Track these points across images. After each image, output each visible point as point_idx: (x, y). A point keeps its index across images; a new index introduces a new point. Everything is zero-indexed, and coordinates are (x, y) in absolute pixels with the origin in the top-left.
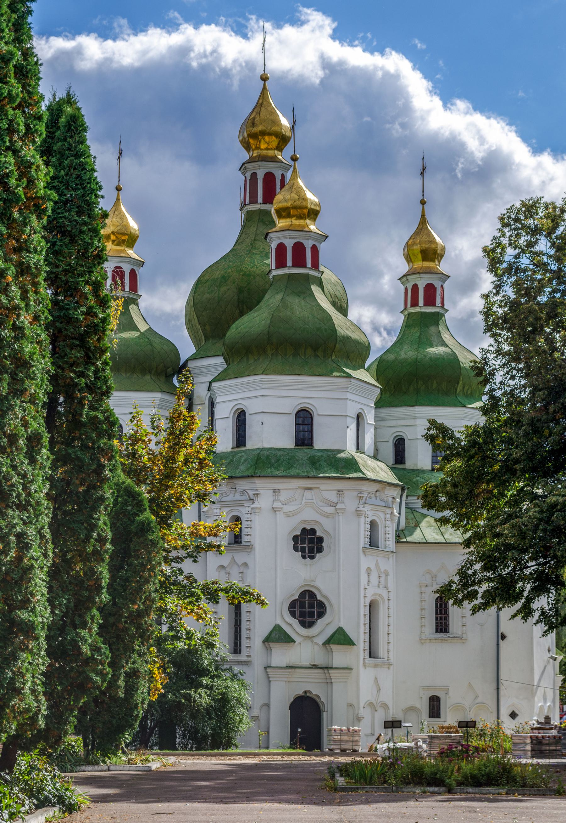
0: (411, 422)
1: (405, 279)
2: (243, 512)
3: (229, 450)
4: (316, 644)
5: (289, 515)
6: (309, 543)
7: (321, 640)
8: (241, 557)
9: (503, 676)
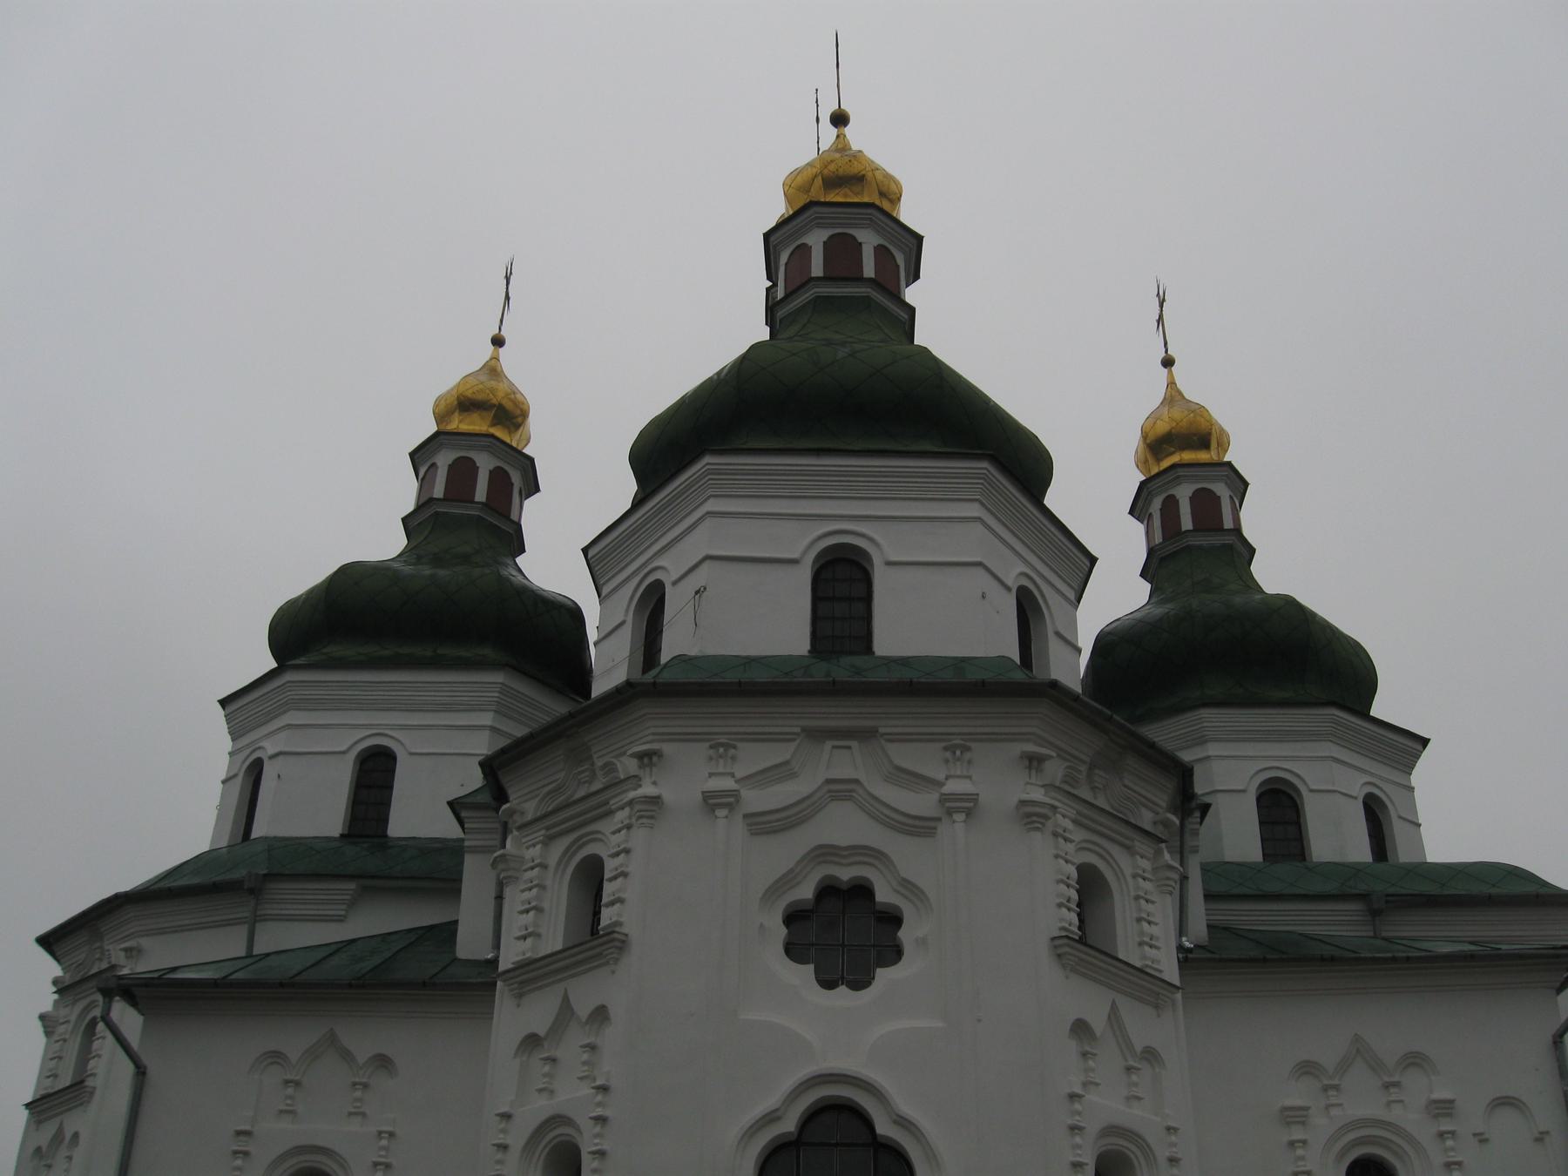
1: (1144, 495)
2: (607, 840)
8: (586, 992)
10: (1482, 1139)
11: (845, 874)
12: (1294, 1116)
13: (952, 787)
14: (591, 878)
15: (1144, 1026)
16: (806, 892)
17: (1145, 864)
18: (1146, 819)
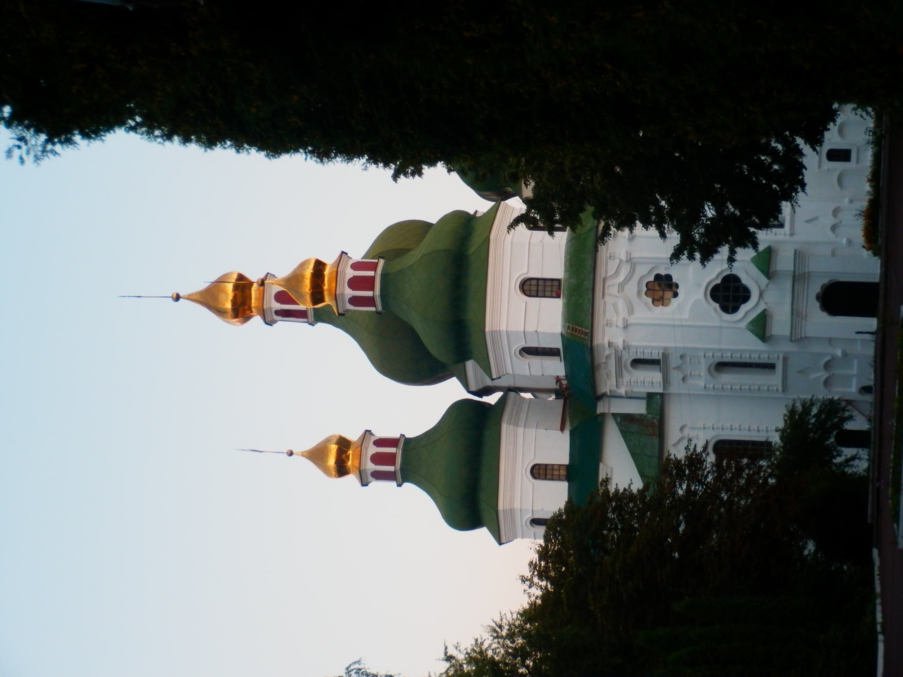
2: (628, 358)
3: (563, 364)
4: (767, 286)
5: (631, 311)
7: (764, 280)
8: (674, 361)
11: (645, 289)
13: (623, 257)
14: (637, 363)
16: (650, 300)
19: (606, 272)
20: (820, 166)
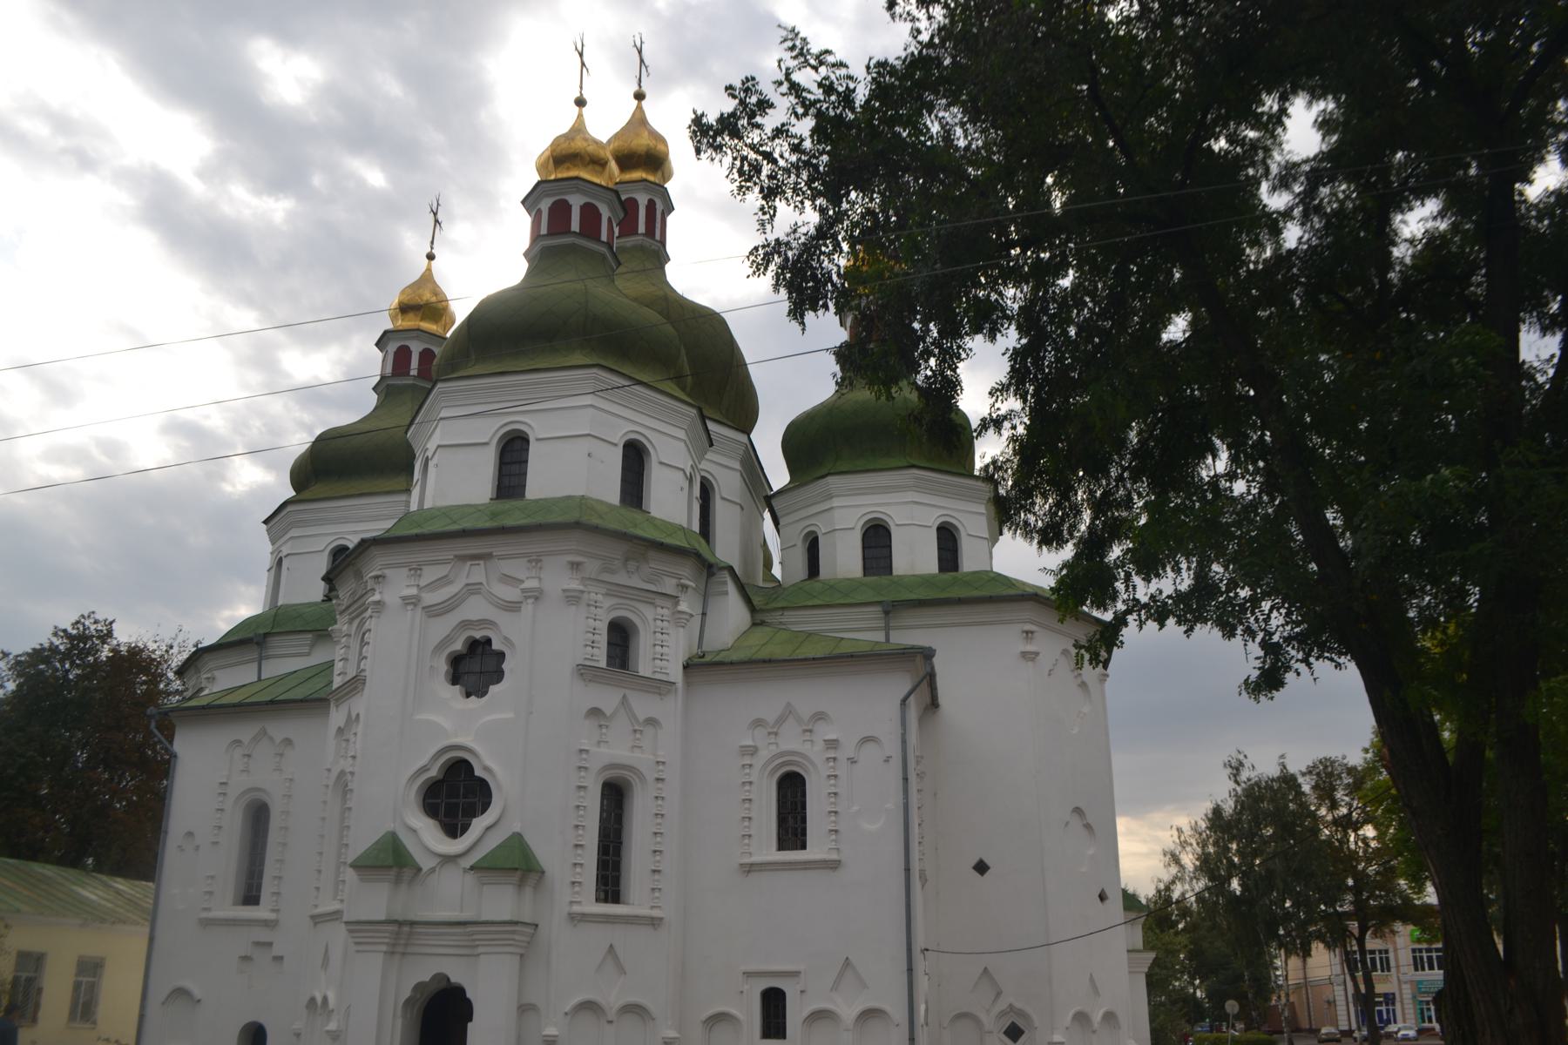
0: (826, 506)
5: (434, 612)
6: (475, 666)
9: (920, 941)
10: (852, 761)
11: (478, 635)
12: (753, 751)
13: (529, 584)
15: (644, 706)
16: (458, 646)
17: (665, 611)
18: (669, 586)
19: (501, 558)
20: (748, 974)
